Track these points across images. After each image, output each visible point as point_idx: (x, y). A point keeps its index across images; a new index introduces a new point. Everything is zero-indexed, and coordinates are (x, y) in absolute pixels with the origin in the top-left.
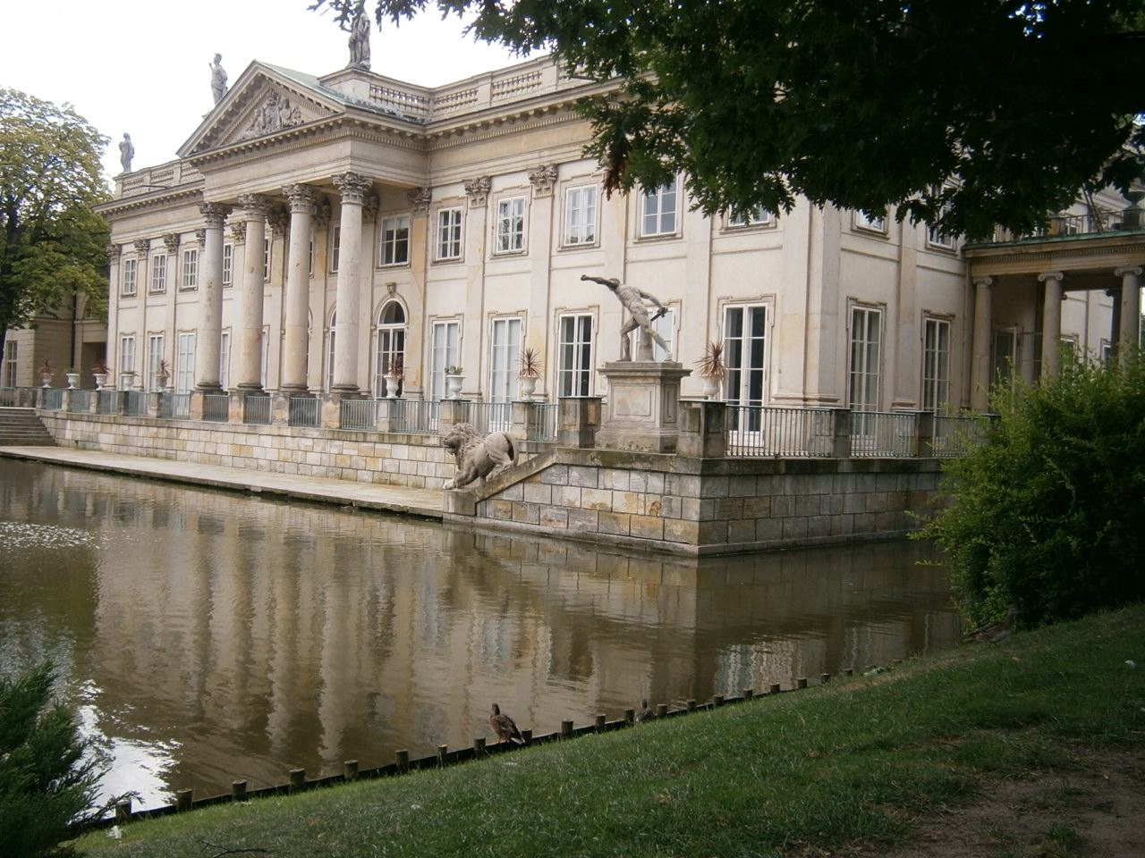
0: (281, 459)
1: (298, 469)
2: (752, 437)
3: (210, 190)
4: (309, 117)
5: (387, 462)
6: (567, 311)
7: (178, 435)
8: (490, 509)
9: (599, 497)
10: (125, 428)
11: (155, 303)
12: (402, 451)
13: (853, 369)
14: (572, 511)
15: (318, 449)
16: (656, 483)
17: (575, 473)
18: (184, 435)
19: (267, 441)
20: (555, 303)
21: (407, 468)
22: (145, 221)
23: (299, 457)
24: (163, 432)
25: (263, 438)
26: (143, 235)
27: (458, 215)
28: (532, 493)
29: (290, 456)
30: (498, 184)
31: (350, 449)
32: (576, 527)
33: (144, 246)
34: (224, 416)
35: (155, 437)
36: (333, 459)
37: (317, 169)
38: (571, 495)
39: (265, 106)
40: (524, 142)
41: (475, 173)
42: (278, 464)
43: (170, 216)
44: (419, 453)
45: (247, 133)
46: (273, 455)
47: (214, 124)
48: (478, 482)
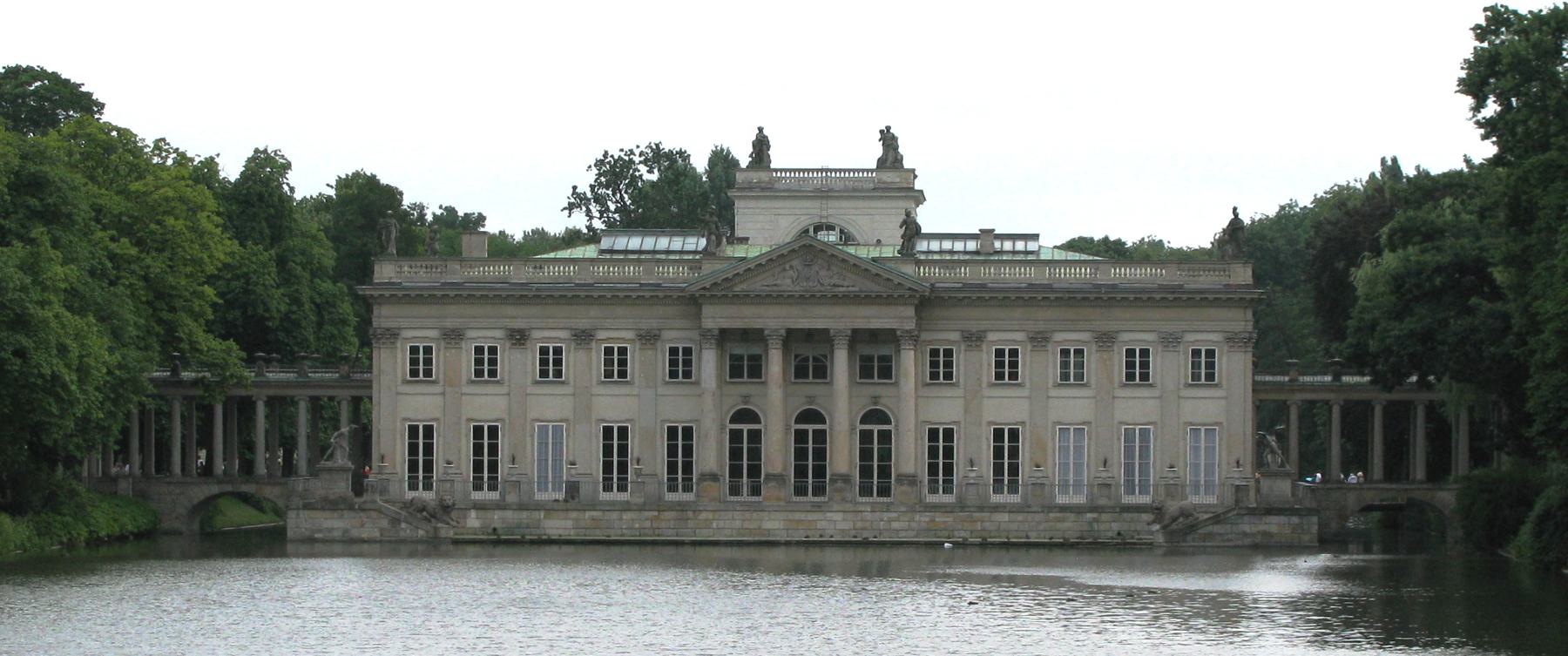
8: (1189, 538)
9: (1262, 528)
14: (1245, 534)
16: (1295, 520)
17: (1246, 518)
19: (838, 517)
22: (453, 309)
26: (449, 323)
27: (948, 353)
28: (1217, 529)
30: (992, 337)
32: (1248, 541)
35: (657, 518)
38: (1247, 528)
39: (795, 263)
40: (1018, 313)
41: (974, 326)
43: (509, 310)
45: (786, 283)
46: (841, 526)
47: (741, 271)
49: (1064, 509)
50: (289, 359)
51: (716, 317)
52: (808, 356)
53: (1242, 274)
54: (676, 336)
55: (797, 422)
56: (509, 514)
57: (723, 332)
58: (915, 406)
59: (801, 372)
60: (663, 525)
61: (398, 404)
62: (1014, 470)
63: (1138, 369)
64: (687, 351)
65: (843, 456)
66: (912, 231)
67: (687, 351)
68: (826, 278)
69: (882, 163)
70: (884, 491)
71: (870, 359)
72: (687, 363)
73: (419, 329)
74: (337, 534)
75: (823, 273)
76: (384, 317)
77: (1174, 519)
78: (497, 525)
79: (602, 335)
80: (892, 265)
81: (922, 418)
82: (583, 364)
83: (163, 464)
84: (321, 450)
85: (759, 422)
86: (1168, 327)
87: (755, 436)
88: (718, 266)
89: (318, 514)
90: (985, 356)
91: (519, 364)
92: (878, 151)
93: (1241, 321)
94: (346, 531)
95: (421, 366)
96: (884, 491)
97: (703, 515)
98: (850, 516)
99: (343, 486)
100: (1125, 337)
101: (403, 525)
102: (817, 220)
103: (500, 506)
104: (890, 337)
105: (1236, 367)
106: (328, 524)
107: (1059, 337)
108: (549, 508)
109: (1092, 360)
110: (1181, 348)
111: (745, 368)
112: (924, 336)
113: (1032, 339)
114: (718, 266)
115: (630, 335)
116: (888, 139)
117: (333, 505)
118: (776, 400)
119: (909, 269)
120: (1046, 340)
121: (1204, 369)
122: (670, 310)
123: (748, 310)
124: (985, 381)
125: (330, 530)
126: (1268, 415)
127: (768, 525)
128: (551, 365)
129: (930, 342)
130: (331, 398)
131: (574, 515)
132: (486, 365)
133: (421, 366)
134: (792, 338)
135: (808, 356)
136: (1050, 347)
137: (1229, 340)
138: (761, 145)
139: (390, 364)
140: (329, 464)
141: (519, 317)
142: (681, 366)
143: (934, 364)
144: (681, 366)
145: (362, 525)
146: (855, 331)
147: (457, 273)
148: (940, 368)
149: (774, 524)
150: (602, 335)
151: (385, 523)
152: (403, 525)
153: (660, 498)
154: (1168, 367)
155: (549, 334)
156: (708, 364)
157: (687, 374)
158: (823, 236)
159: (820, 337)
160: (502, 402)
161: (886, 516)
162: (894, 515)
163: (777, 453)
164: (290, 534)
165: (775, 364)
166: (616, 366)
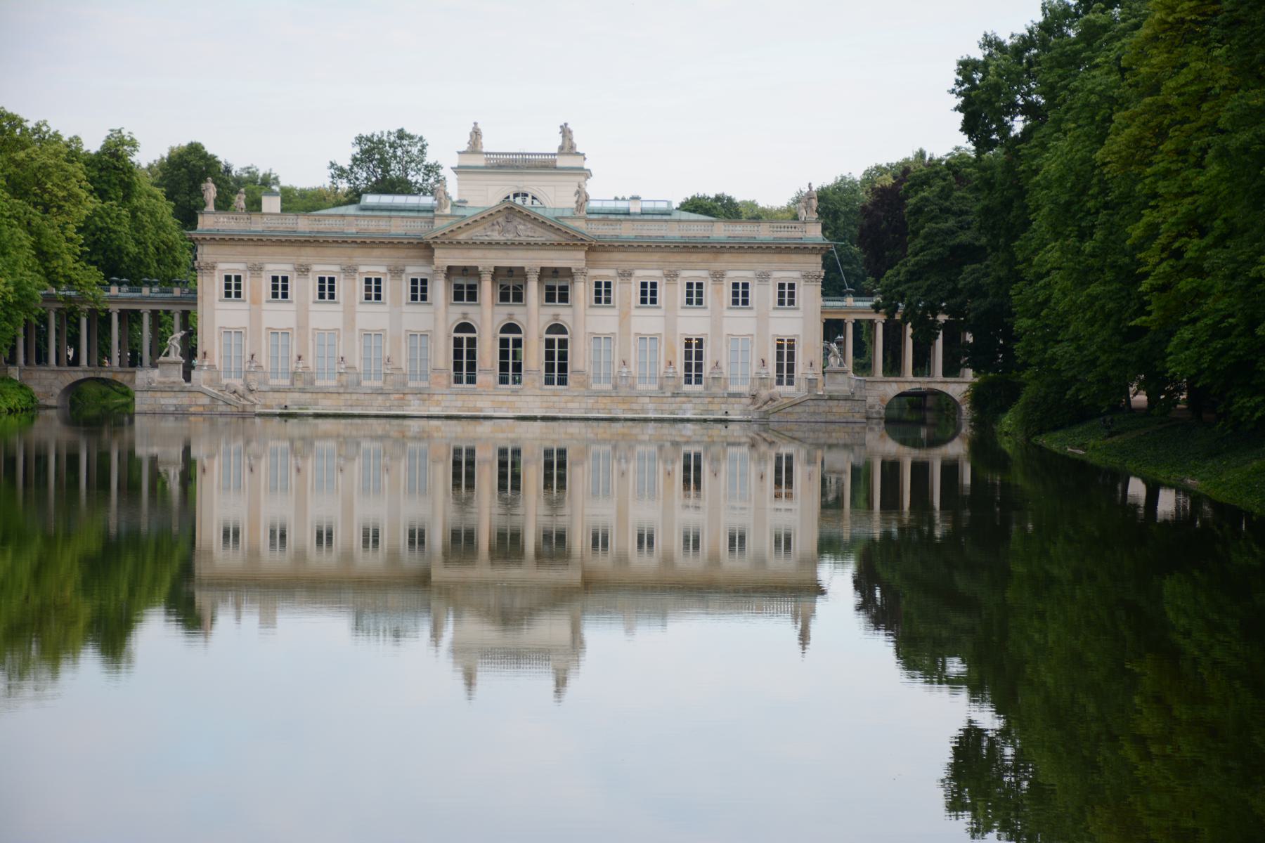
4: (555, 238)
19: (528, 399)
20: (680, 331)
23: (563, 405)
27: (608, 284)
30: (638, 273)
33: (256, 270)
40: (656, 257)
41: (625, 266)
45: (496, 236)
48: (765, 408)
49: (687, 395)
50: (135, 284)
51: (445, 258)
52: (510, 287)
53: (814, 233)
54: (416, 270)
55: (503, 331)
56: (296, 395)
57: (449, 268)
58: (585, 320)
59: (504, 298)
61: (218, 316)
62: (791, 369)
63: (741, 295)
64: (424, 282)
65: (533, 356)
66: (582, 197)
67: (424, 282)
68: (525, 231)
69: (561, 148)
70: (563, 381)
71: (554, 288)
72: (424, 290)
73: (228, 263)
75: (521, 227)
76: (206, 254)
77: (766, 403)
78: (288, 403)
79: (363, 269)
80: (569, 223)
81: (589, 330)
82: (350, 289)
83: (42, 358)
84: (158, 348)
85: (472, 330)
86: (762, 268)
87: (472, 342)
88: (446, 222)
90: (633, 287)
91: (302, 288)
92: (558, 140)
93: (815, 265)
95: (233, 288)
96: (563, 381)
97: (436, 397)
98: (538, 399)
99: (176, 375)
100: (730, 274)
102: (515, 190)
103: (289, 390)
104: (568, 273)
105: (810, 296)
107: (685, 274)
108: (326, 392)
109: (708, 290)
110: (771, 282)
111: (465, 292)
112: (593, 272)
113: (667, 276)
114: (446, 222)
115: (383, 269)
116: (565, 132)
117: (170, 389)
118: (488, 316)
119: (580, 225)
120: (677, 276)
121: (786, 295)
122: (413, 252)
123: (466, 253)
124: (633, 305)
126: (832, 329)
127: (480, 404)
128: (327, 289)
129: (595, 277)
130: (167, 312)
132: (280, 288)
133: (233, 288)
134: (497, 273)
135: (510, 287)
136: (679, 280)
137: (804, 277)
138: (476, 134)
139: (210, 288)
140: (167, 359)
141: (306, 255)
142: (419, 291)
143: (598, 292)
144: (419, 291)
146: (542, 269)
147: (257, 225)
148: (602, 293)
149: (484, 405)
150: (363, 269)
153: (405, 384)
154: (765, 295)
155: (325, 266)
156: (439, 290)
157: (424, 298)
158: (519, 201)
159: (518, 274)
161: (563, 399)
163: (488, 354)
164: (137, 408)
165: (487, 290)
166: (374, 290)
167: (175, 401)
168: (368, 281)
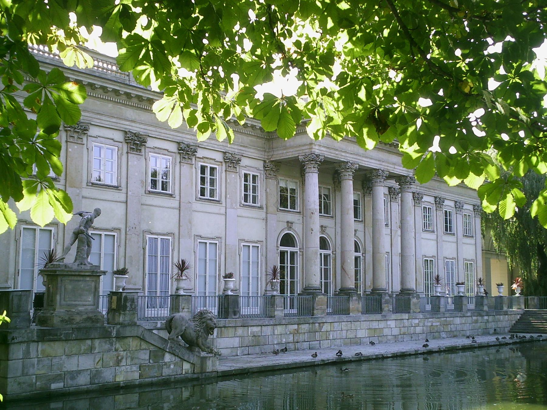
0: (401, 333)
1: (412, 338)
2: (246, 310)
3: (320, 146)
5: (452, 326)
6: (426, 257)
7: (321, 328)
10: (256, 329)
11: (102, 197)
12: (458, 320)
13: (326, 278)
15: (421, 324)
18: (326, 327)
21: (459, 328)
24: (305, 327)
25: (389, 323)
29: (406, 331)
31: (436, 322)
34: (346, 311)
35: (297, 332)
36: (429, 329)
37: (396, 167)
42: (400, 336)
44: (463, 320)
46: (396, 332)
60: (301, 338)
74: (83, 381)
89: (57, 348)
94: (95, 374)
101: (168, 358)
106: (71, 365)
125: (74, 374)
131: (240, 331)
145: (118, 362)
151: (144, 356)
152: (168, 358)
160: (120, 209)
162: (417, 321)
167: (86, 363)
168: (203, 169)
